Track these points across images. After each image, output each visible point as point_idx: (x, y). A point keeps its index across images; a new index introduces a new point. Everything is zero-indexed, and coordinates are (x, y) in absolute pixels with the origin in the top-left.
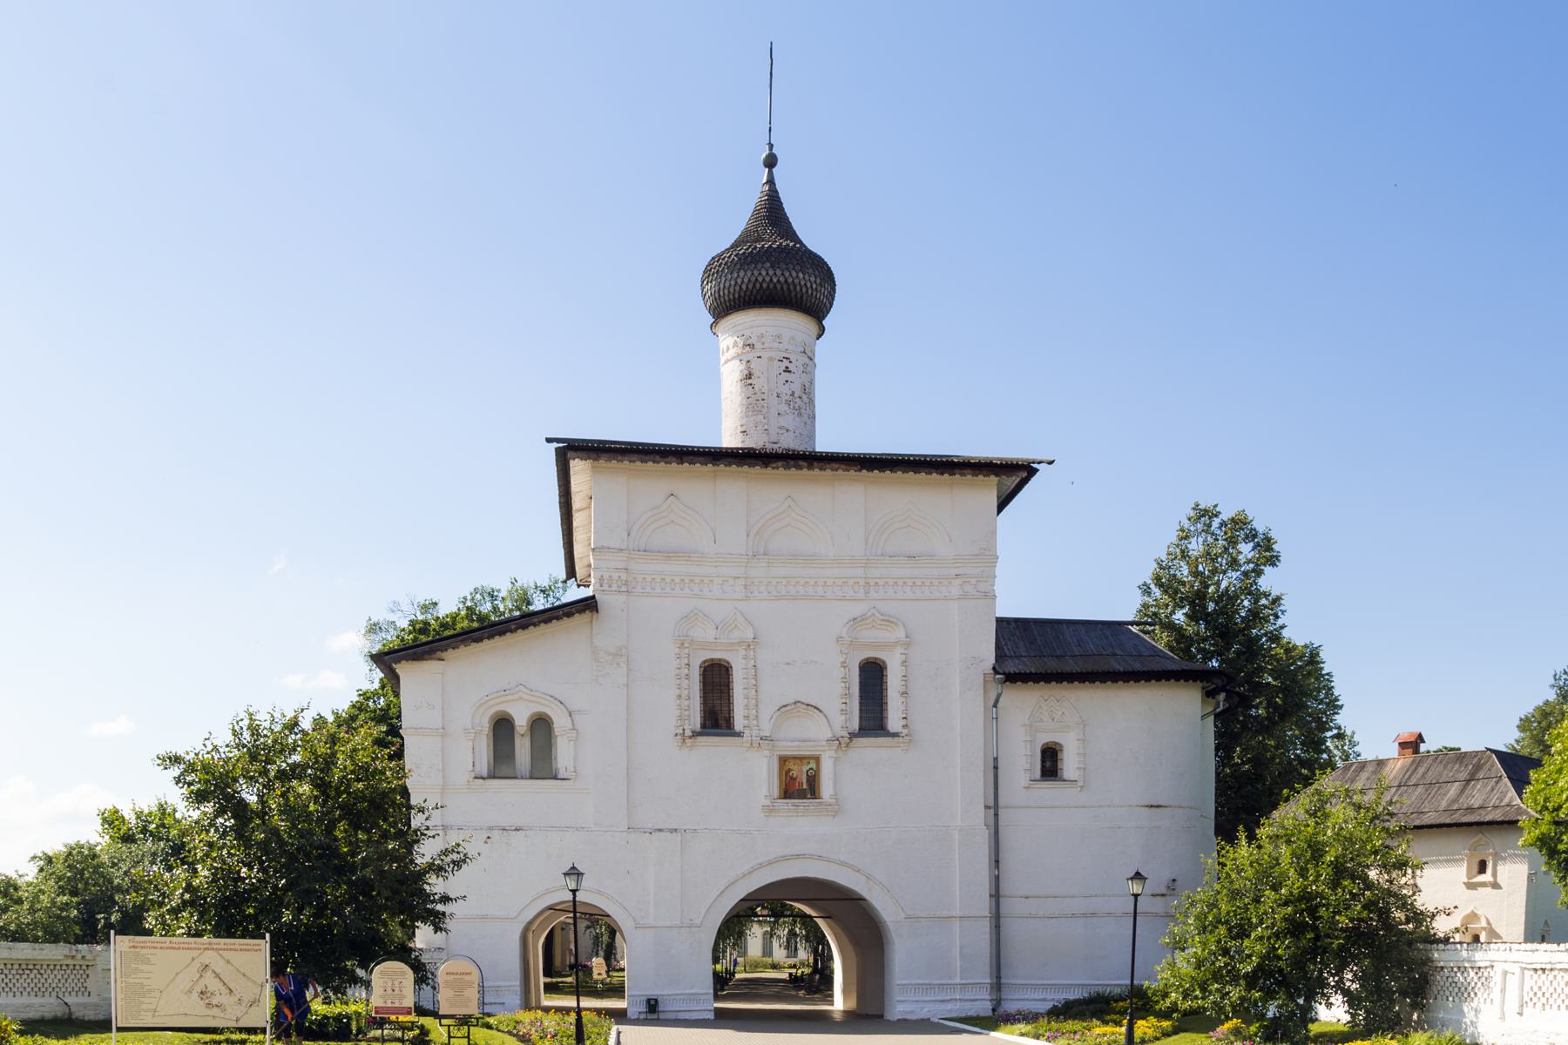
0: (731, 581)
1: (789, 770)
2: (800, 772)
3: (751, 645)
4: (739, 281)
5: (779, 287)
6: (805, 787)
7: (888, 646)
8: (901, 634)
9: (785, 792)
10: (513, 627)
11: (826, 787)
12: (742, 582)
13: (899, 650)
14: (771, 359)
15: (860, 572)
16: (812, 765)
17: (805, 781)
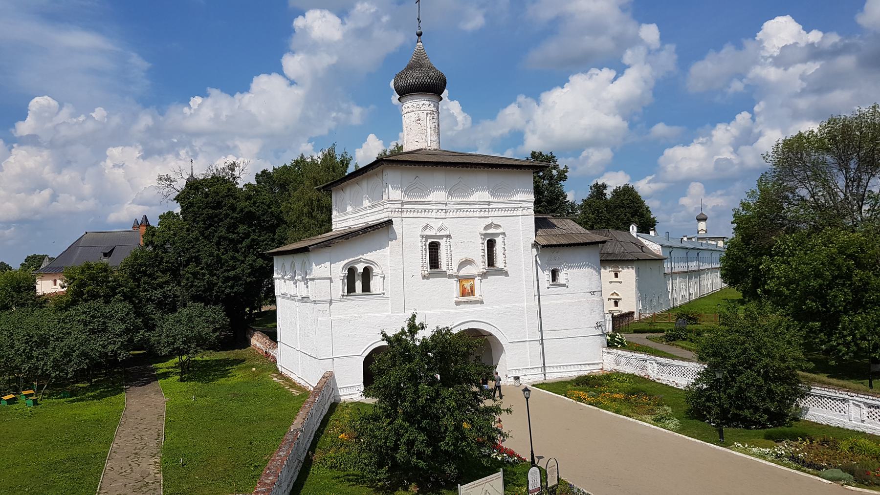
0: (440, 211)
1: (464, 285)
2: (467, 285)
3: (449, 236)
4: (416, 83)
5: (431, 86)
6: (469, 291)
7: (498, 235)
8: (500, 231)
9: (463, 294)
10: (361, 233)
11: (477, 292)
12: (444, 211)
13: (501, 236)
14: (427, 114)
15: (487, 206)
16: (472, 282)
17: (469, 289)
